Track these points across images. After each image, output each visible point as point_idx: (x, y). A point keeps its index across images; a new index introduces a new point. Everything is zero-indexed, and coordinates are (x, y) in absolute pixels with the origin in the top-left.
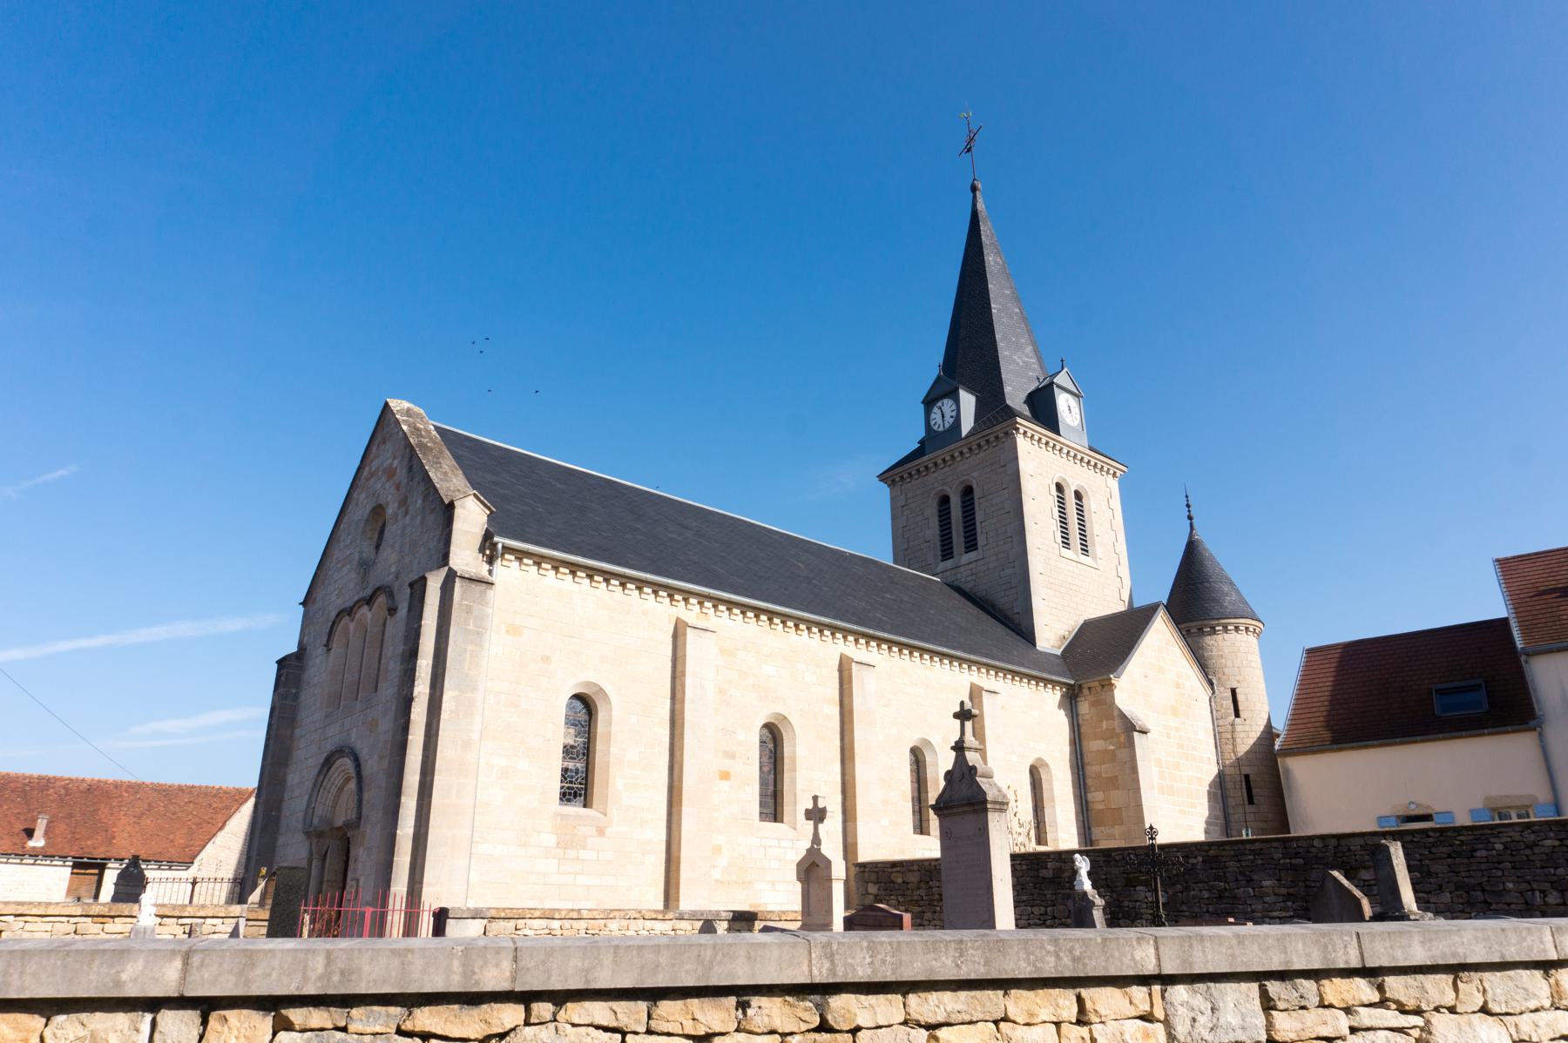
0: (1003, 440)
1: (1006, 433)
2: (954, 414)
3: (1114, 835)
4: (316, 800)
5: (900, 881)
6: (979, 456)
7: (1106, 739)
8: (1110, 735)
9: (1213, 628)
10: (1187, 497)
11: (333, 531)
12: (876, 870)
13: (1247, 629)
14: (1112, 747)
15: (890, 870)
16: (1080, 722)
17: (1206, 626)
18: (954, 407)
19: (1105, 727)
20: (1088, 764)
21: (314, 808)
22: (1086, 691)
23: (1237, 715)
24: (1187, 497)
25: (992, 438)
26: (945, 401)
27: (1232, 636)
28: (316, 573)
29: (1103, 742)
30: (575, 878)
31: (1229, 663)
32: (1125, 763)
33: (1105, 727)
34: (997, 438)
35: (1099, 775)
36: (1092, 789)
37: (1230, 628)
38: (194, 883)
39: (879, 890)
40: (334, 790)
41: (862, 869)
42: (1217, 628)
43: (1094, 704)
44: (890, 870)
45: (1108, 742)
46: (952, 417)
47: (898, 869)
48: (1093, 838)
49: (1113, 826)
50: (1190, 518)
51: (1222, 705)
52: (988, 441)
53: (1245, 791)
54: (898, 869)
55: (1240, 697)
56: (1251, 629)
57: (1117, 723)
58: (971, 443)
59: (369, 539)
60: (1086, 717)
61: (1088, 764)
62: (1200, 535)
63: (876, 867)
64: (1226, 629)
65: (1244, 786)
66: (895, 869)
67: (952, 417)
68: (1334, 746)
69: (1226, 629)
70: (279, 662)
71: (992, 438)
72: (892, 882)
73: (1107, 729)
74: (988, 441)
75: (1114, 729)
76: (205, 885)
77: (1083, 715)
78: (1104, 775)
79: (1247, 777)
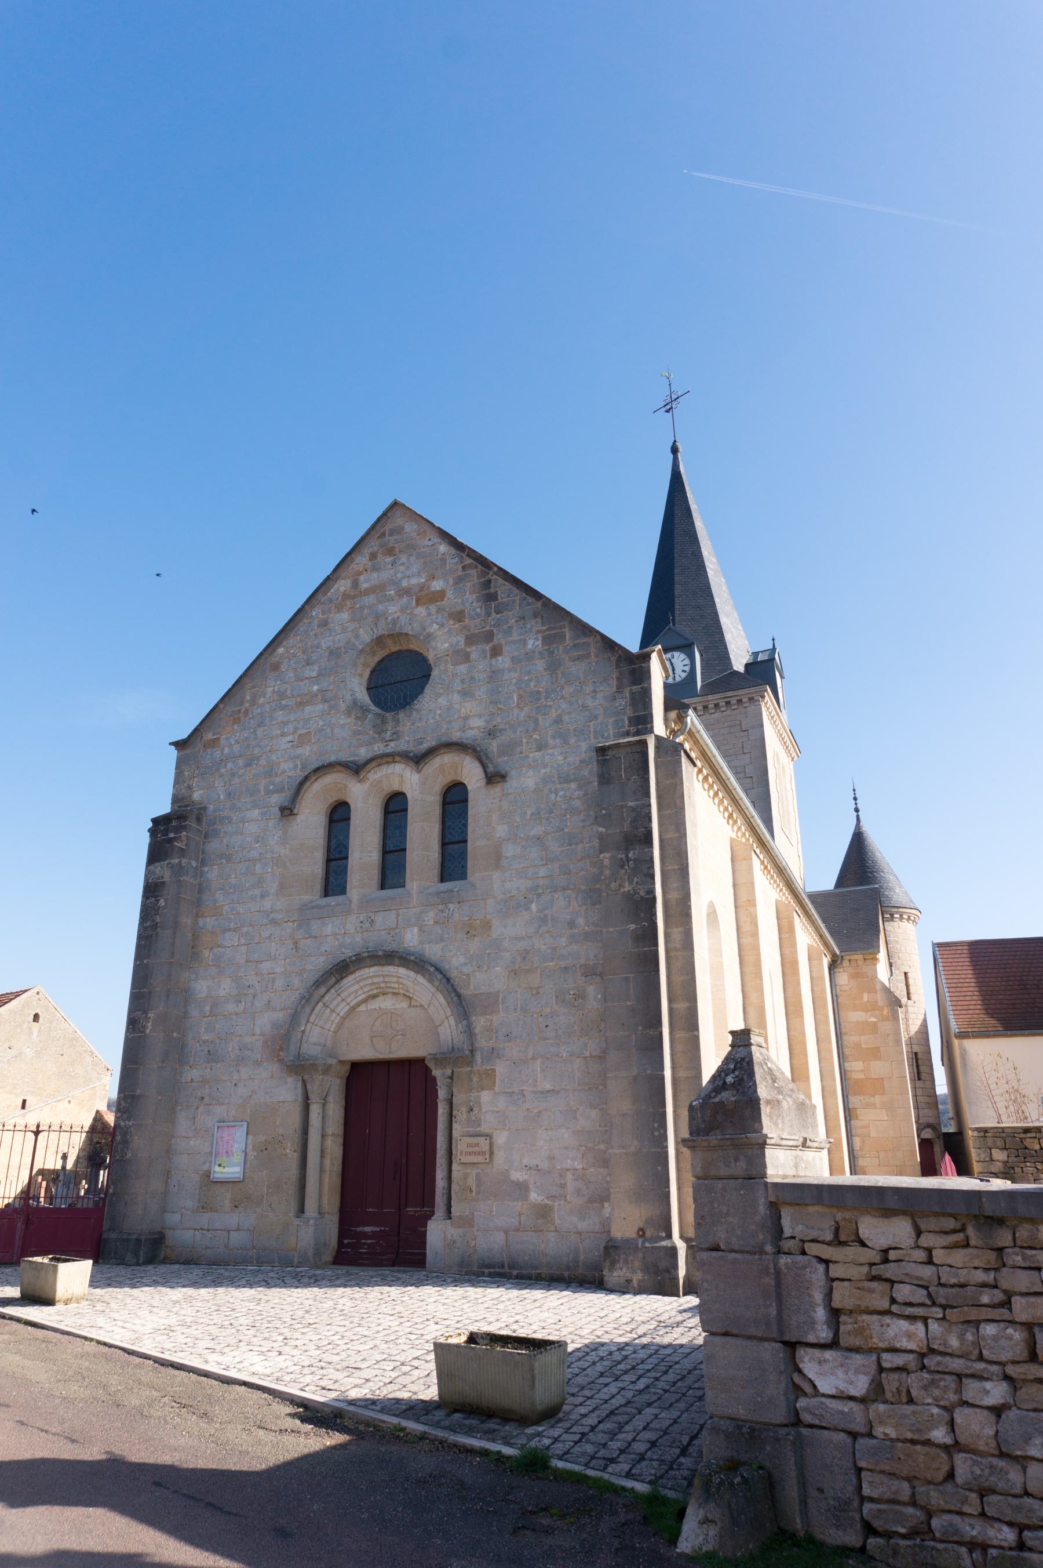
0: (745, 705)
1: (751, 699)
2: (687, 669)
3: (875, 1104)
4: (308, 1021)
5: (1037, 1147)
6: (713, 715)
7: (866, 1011)
8: (873, 1007)
9: (892, 915)
10: (854, 790)
11: (261, 654)
12: (1004, 1135)
13: (901, 916)
14: (874, 1020)
15: (1022, 1136)
16: (838, 992)
17: (897, 913)
18: (687, 662)
19: (865, 999)
20: (846, 1034)
21: (303, 1032)
22: (846, 963)
23: (909, 998)
24: (854, 790)
25: (734, 701)
26: (676, 654)
27: (905, 925)
28: (216, 706)
29: (863, 1014)
30: (32, 1131)
31: (903, 948)
32: (888, 1035)
33: (865, 999)
34: (740, 701)
35: (858, 1045)
36: (850, 1059)
37: (895, 916)
38: (37, 1133)
39: (1008, 1157)
40: (343, 1009)
41: (982, 1134)
42: (895, 916)
43: (855, 976)
44: (1022, 1136)
45: (869, 1013)
46: (684, 671)
47: (1033, 1135)
48: (851, 1107)
49: (873, 1096)
50: (857, 810)
51: (897, 987)
52: (728, 703)
53: (915, 1067)
54: (1033, 1135)
55: (911, 981)
56: (912, 918)
57: (880, 998)
58: (708, 701)
59: (359, 675)
60: (843, 988)
61: (846, 1034)
62: (867, 828)
63: (1003, 1132)
64: (901, 918)
65: (915, 1064)
66: (1029, 1135)
67: (684, 671)
68: (1009, 1032)
69: (901, 918)
70: (155, 821)
71: (734, 701)
72: (1026, 1148)
73: (868, 1001)
74: (728, 703)
75: (877, 1002)
76: (54, 1136)
77: (841, 986)
78: (863, 1046)
79: (916, 1054)
